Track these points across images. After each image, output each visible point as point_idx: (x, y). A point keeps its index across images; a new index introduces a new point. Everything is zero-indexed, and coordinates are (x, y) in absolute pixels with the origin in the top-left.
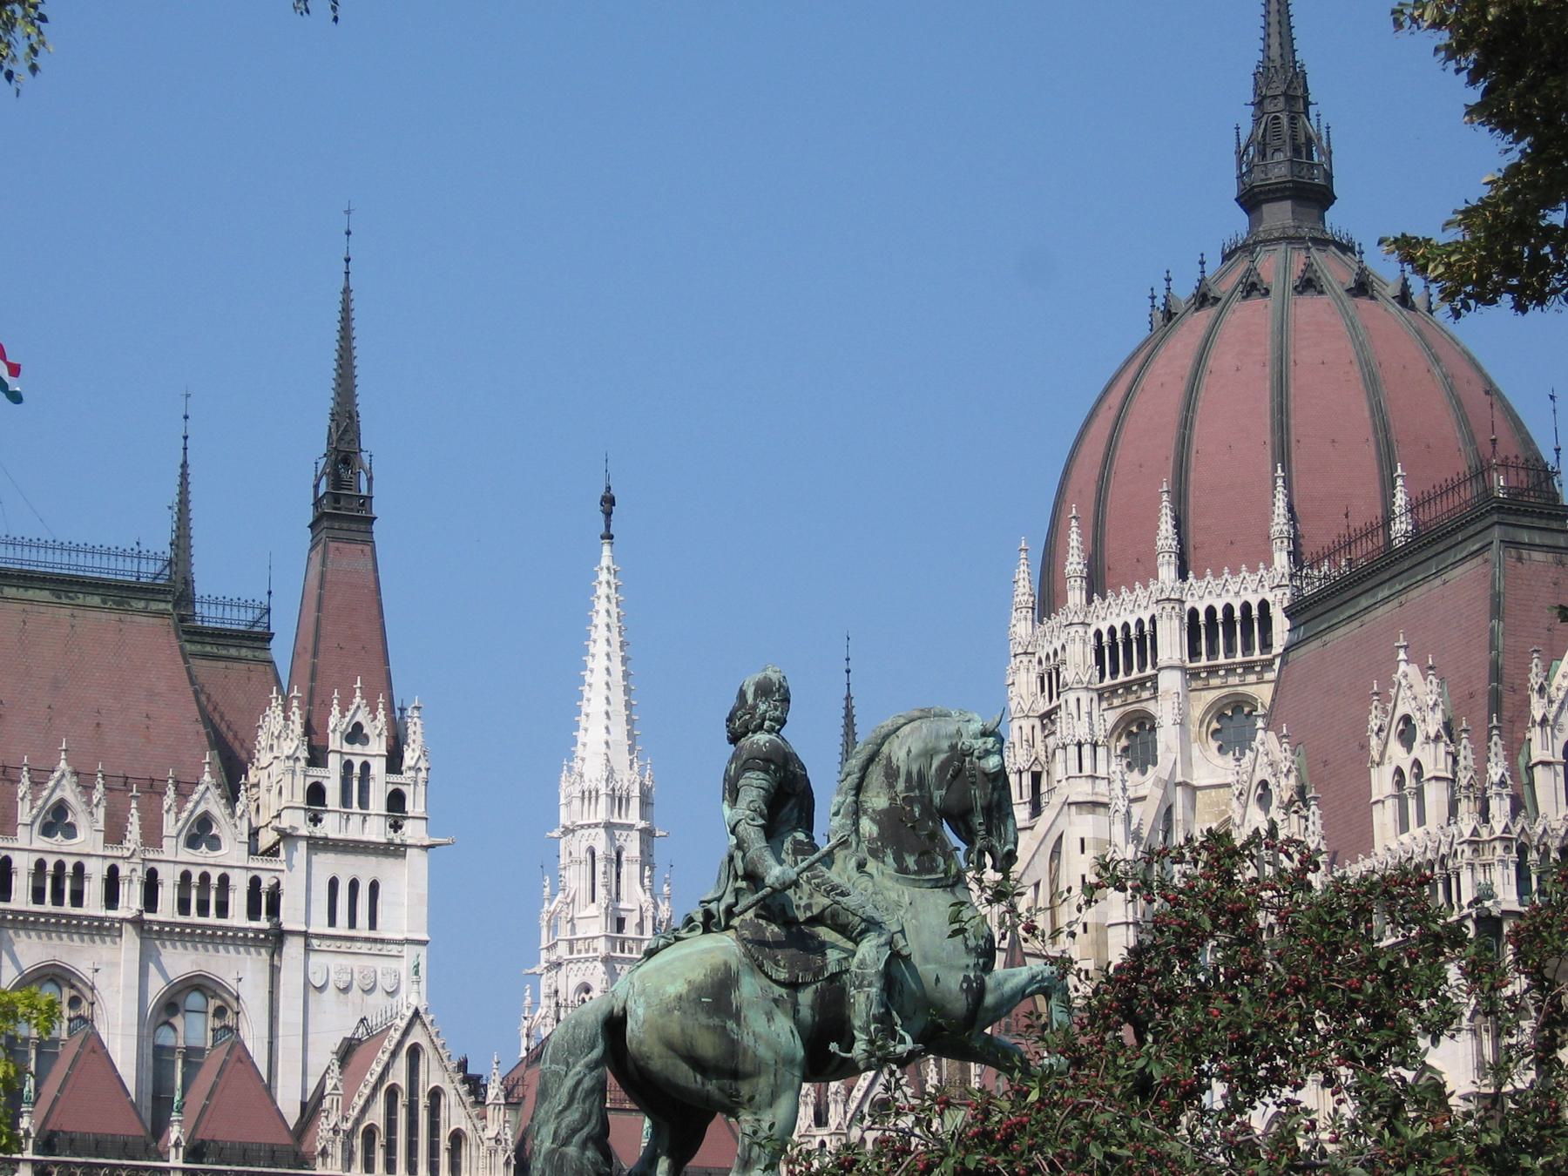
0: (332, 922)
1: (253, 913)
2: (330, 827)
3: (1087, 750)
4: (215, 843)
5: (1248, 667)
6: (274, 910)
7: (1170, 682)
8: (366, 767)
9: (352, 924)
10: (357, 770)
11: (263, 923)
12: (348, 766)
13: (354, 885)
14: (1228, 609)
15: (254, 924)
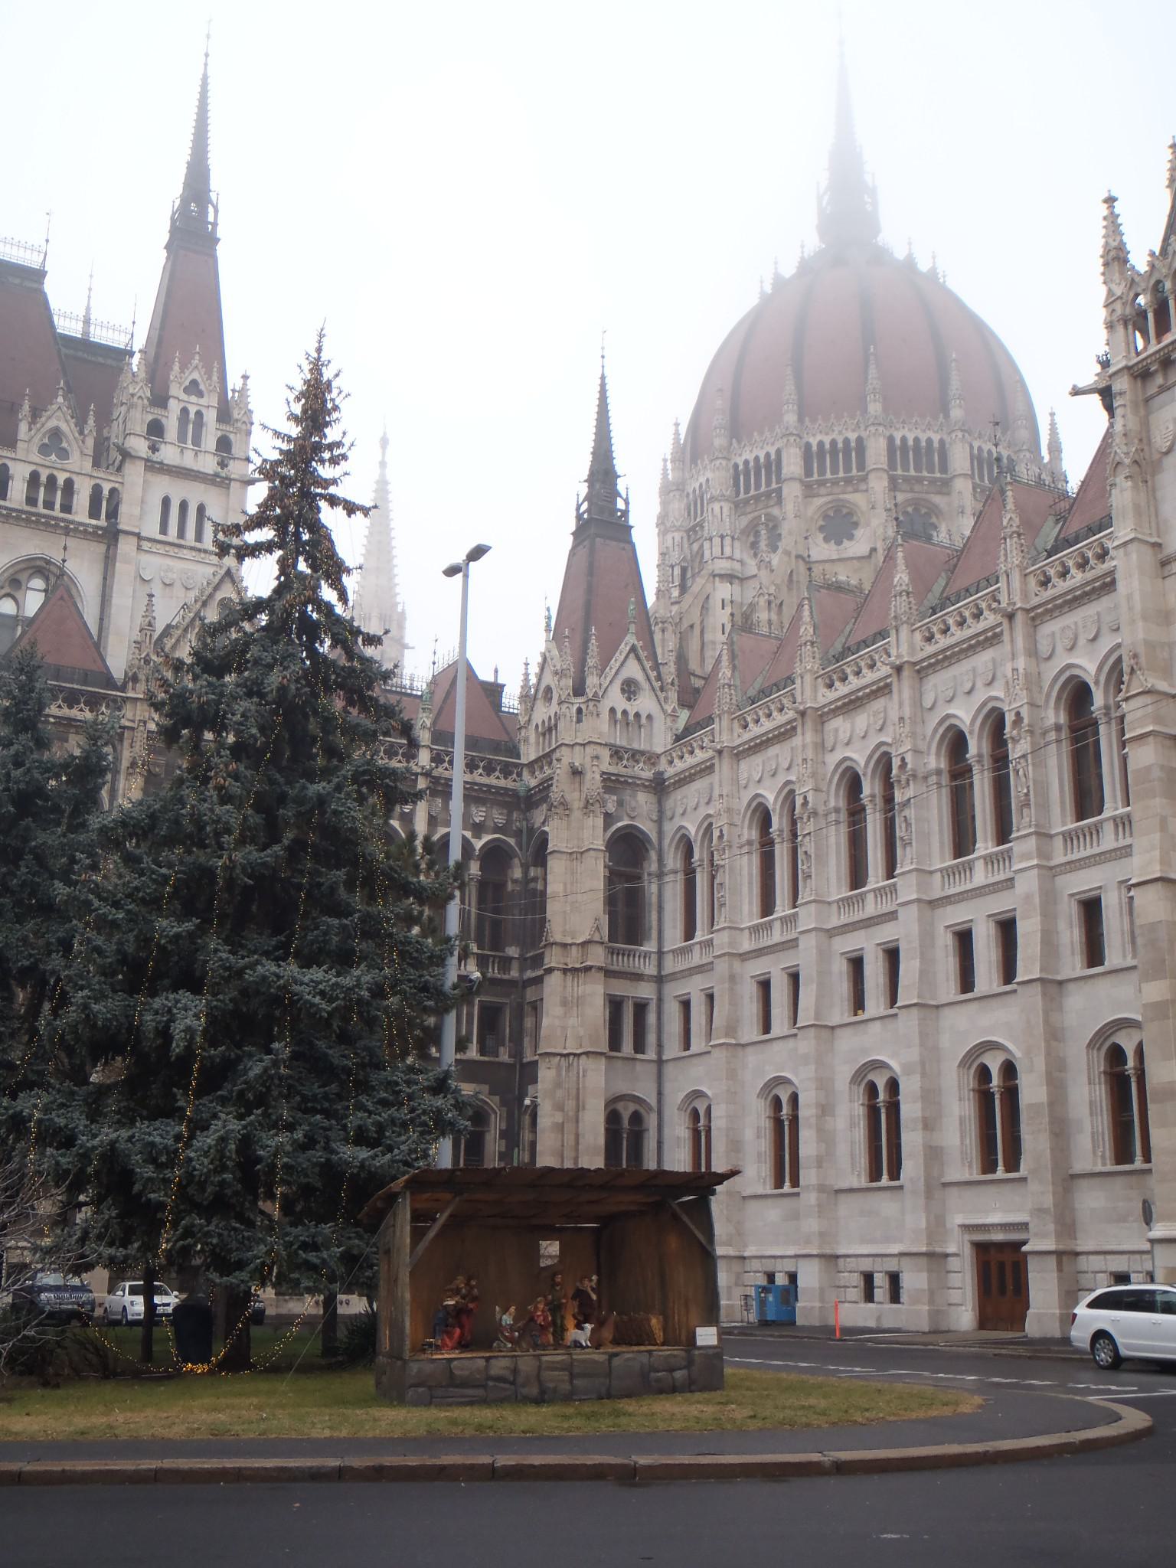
0: (164, 530)
1: (94, 513)
2: (169, 454)
3: (728, 541)
4: (64, 454)
5: (848, 481)
6: (113, 514)
7: (792, 491)
8: (199, 414)
9: (181, 533)
10: (192, 416)
11: (102, 522)
12: (185, 411)
13: (184, 506)
14: (833, 443)
15: (94, 522)
